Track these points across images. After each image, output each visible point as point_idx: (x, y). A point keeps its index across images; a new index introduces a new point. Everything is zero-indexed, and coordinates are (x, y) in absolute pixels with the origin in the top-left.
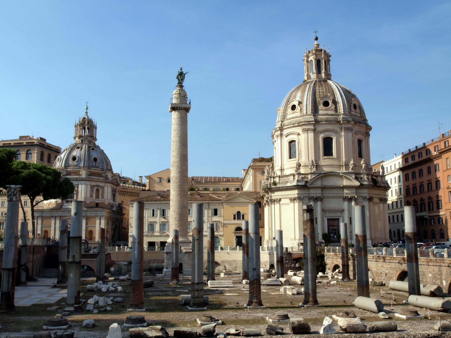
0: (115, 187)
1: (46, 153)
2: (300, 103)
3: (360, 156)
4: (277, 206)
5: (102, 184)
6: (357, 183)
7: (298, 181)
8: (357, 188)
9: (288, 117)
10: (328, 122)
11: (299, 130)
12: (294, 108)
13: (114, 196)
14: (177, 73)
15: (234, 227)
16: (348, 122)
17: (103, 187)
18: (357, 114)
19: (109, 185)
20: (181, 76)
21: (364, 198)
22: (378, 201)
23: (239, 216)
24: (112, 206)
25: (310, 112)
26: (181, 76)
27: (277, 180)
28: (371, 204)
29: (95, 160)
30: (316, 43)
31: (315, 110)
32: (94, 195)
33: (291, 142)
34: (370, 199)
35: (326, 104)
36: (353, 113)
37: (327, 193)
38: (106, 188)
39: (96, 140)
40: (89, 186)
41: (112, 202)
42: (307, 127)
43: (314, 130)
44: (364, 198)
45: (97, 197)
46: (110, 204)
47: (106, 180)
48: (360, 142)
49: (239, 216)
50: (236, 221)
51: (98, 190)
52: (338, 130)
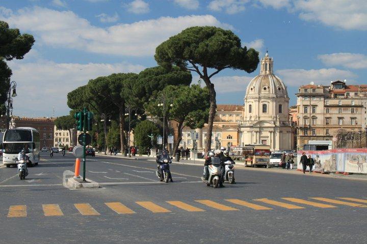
3: (280, 111)
6: (274, 126)
8: (274, 127)
10: (265, 98)
11: (253, 100)
15: (227, 142)
16: (274, 98)
23: (230, 137)
25: (257, 91)
27: (243, 122)
30: (267, 54)
31: (260, 91)
33: (250, 105)
35: (265, 89)
42: (256, 100)
43: (259, 101)
48: (280, 106)
49: (230, 137)
50: (228, 140)
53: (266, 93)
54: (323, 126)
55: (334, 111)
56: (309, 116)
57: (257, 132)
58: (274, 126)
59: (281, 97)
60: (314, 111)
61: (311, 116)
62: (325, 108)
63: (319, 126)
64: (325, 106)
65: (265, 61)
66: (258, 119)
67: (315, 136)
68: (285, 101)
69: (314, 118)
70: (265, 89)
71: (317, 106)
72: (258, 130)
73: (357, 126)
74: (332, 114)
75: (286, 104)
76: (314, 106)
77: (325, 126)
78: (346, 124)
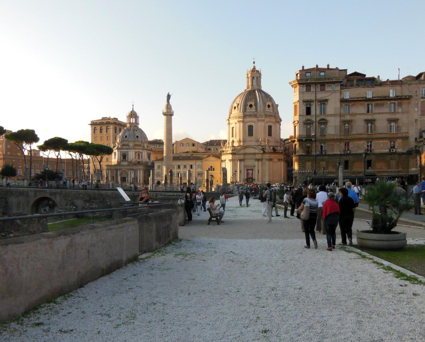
0: (149, 152)
1: (118, 128)
2: (238, 105)
4: (224, 163)
5: (141, 151)
7: (232, 151)
8: (262, 154)
9: (233, 113)
12: (235, 108)
13: (149, 157)
14: (167, 95)
17: (142, 153)
18: (270, 111)
19: (145, 151)
20: (169, 97)
21: (266, 159)
22: (277, 160)
23: (212, 169)
24: (148, 163)
26: (169, 97)
28: (271, 163)
29: (137, 137)
32: (137, 157)
34: (270, 160)
36: (266, 110)
37: (246, 157)
38: (143, 153)
39: (139, 124)
40: (134, 152)
41: (147, 160)
43: (243, 121)
44: (266, 159)
45: (139, 158)
46: (146, 162)
47: (144, 149)
48: (270, 127)
51: (139, 154)
52: (256, 121)
53: (252, 110)
54: (339, 137)
55: (361, 109)
56: (314, 119)
57: (240, 160)
58: (262, 152)
59: (270, 116)
60: (323, 111)
61: (318, 119)
62: (343, 104)
63: (332, 137)
64: (343, 101)
65: (251, 74)
66: (242, 144)
67: (325, 155)
68: (276, 121)
69: (324, 122)
70: (251, 106)
71: (327, 100)
72: (241, 157)
73: (400, 135)
74: (356, 114)
75: (278, 125)
76: (324, 102)
77: (342, 137)
78: (380, 132)
